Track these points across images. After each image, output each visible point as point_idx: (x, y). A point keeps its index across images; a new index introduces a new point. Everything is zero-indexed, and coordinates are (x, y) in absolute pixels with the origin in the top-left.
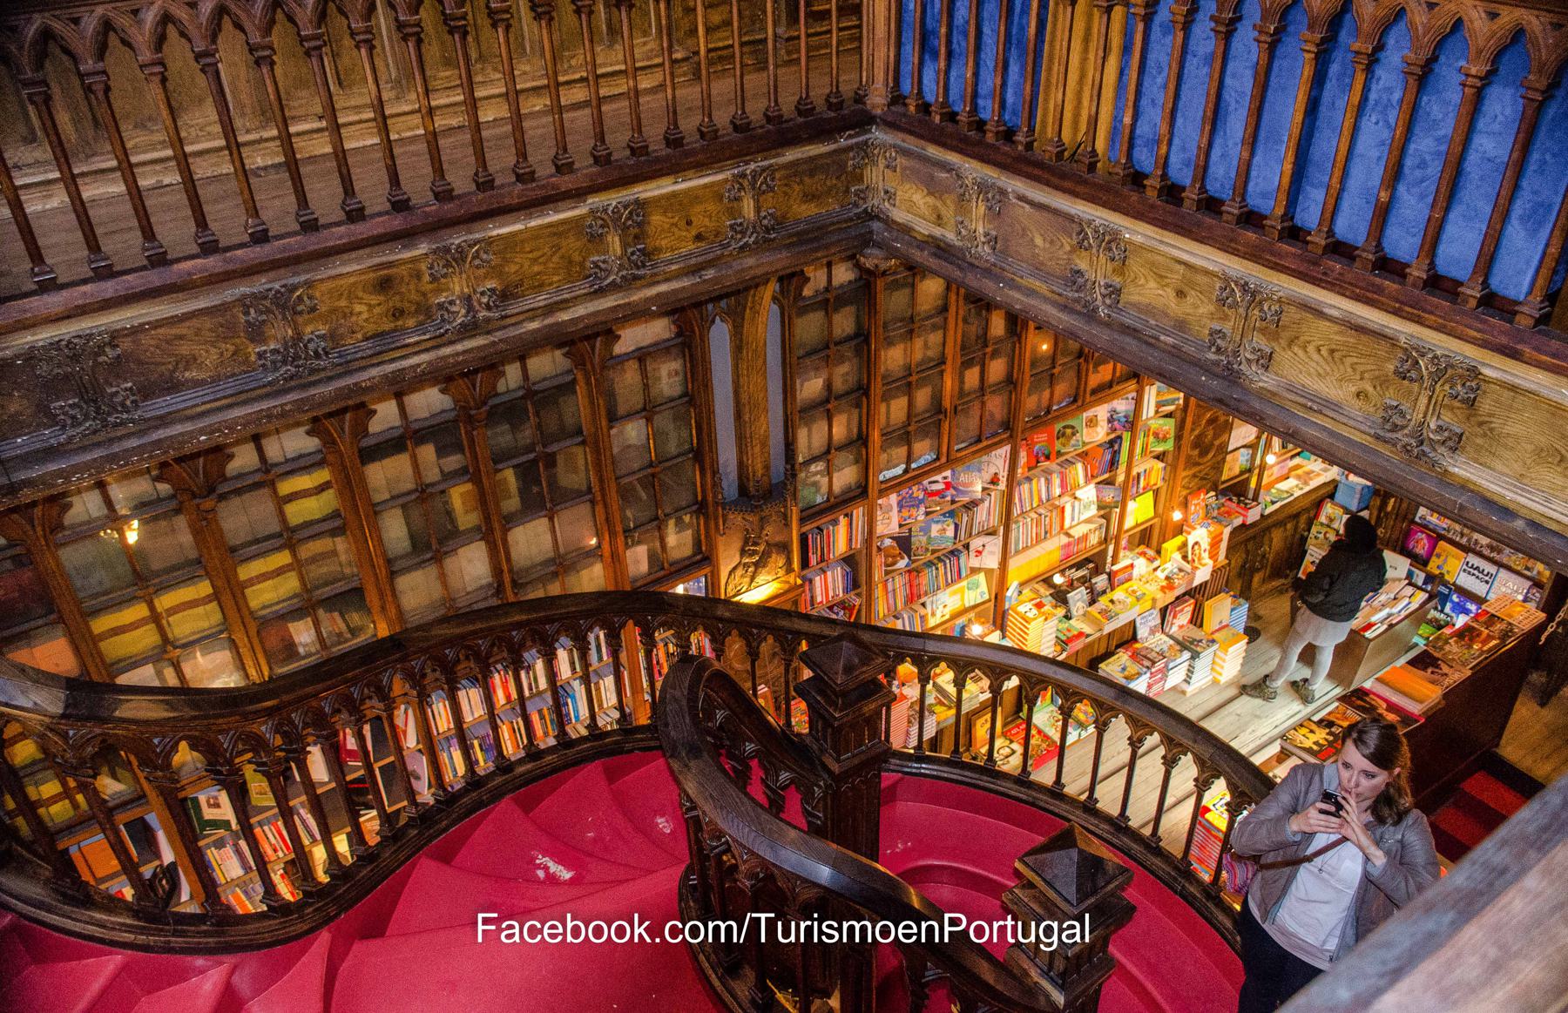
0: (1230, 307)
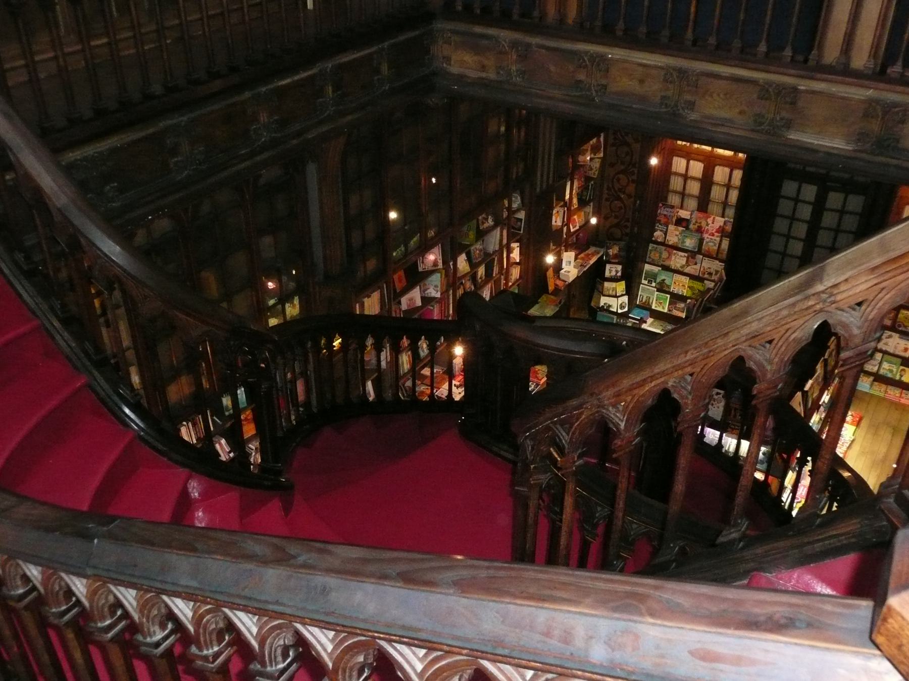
0: (671, 82)
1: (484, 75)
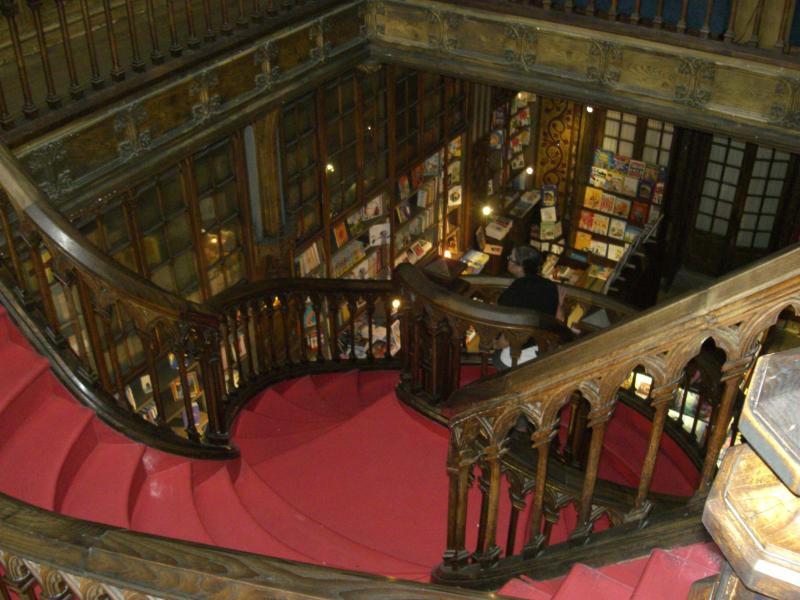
1: (416, 44)
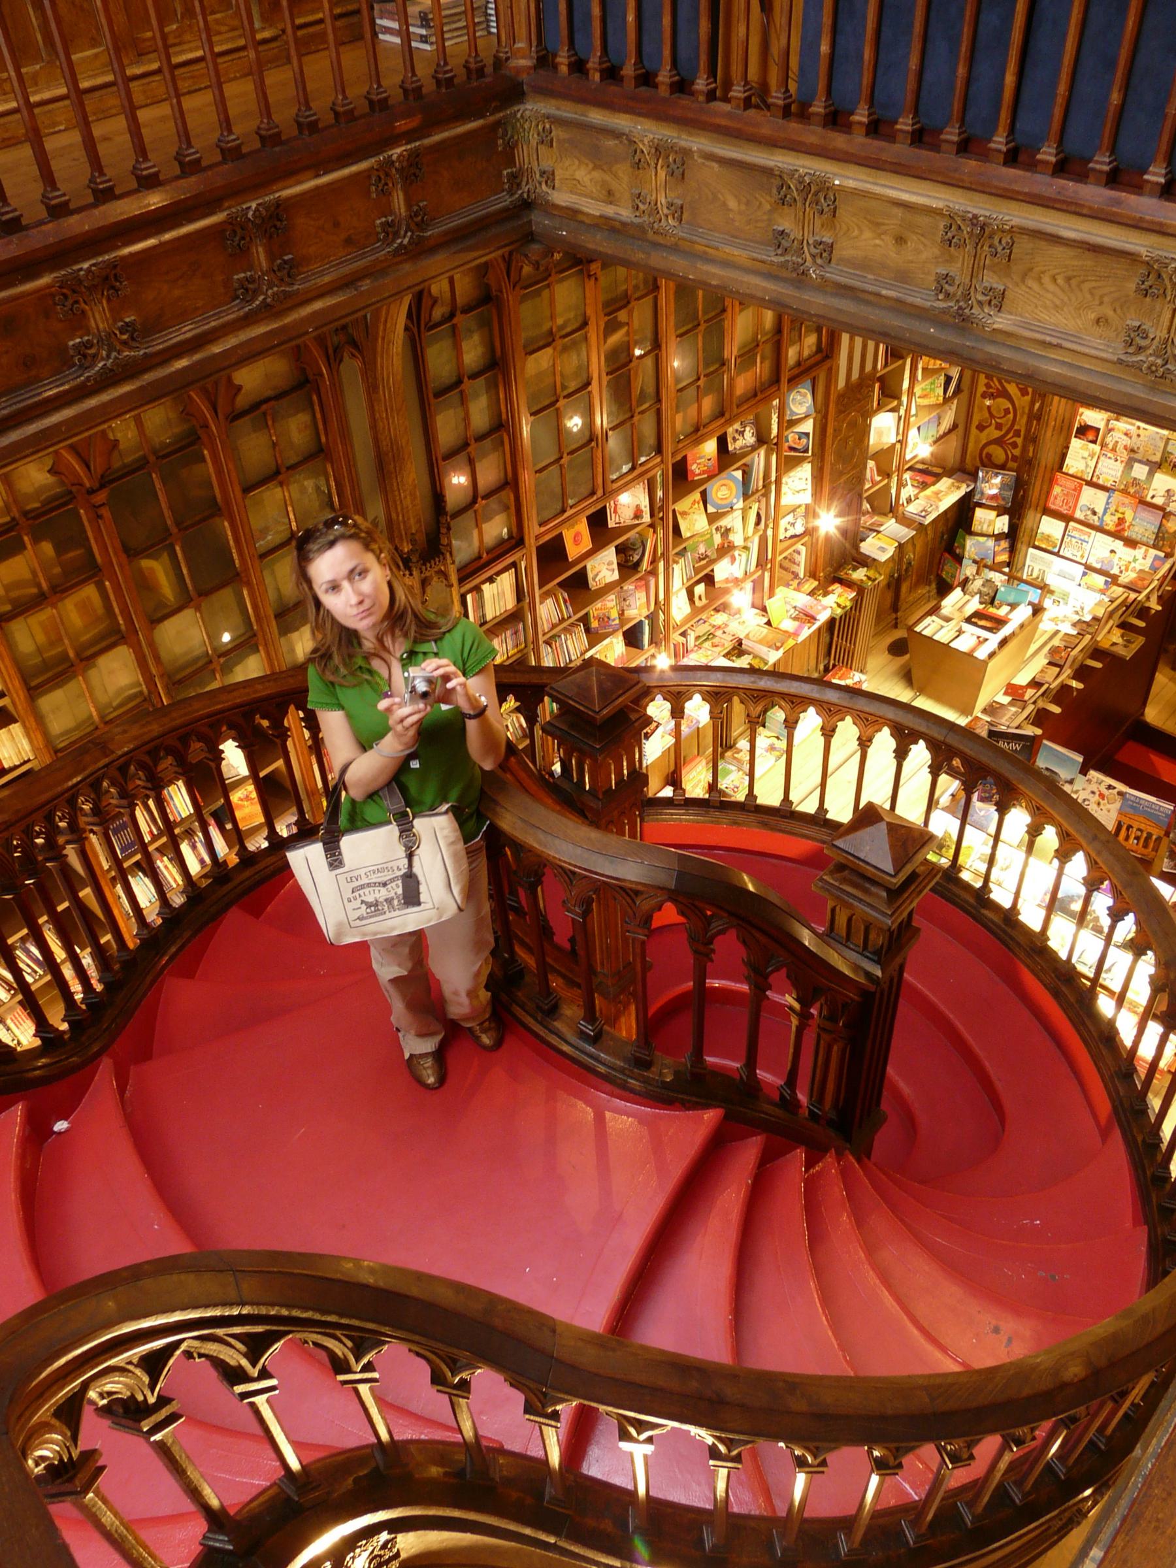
0: (958, 246)
1: (610, 211)
